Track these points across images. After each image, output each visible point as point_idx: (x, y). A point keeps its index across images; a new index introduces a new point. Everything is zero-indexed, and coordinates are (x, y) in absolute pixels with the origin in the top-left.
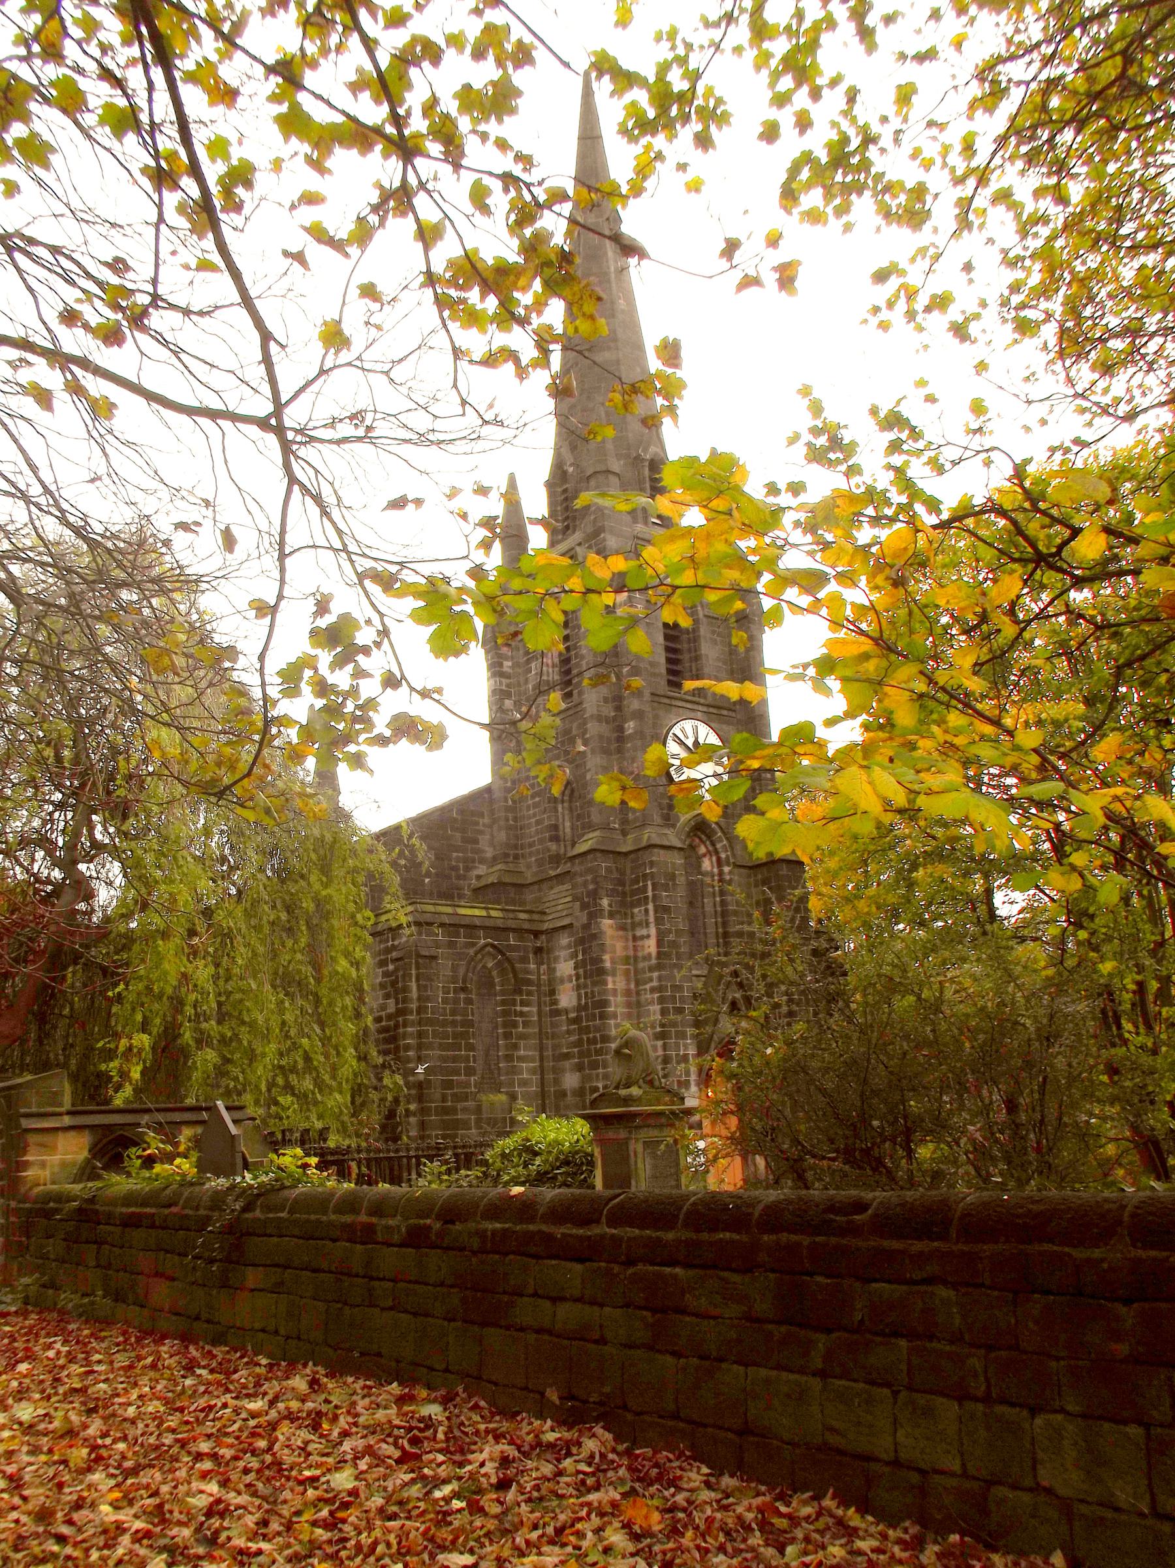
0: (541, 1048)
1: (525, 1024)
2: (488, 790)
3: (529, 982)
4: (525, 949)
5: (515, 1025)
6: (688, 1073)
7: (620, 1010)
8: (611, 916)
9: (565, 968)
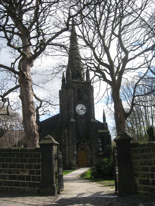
9: (63, 136)
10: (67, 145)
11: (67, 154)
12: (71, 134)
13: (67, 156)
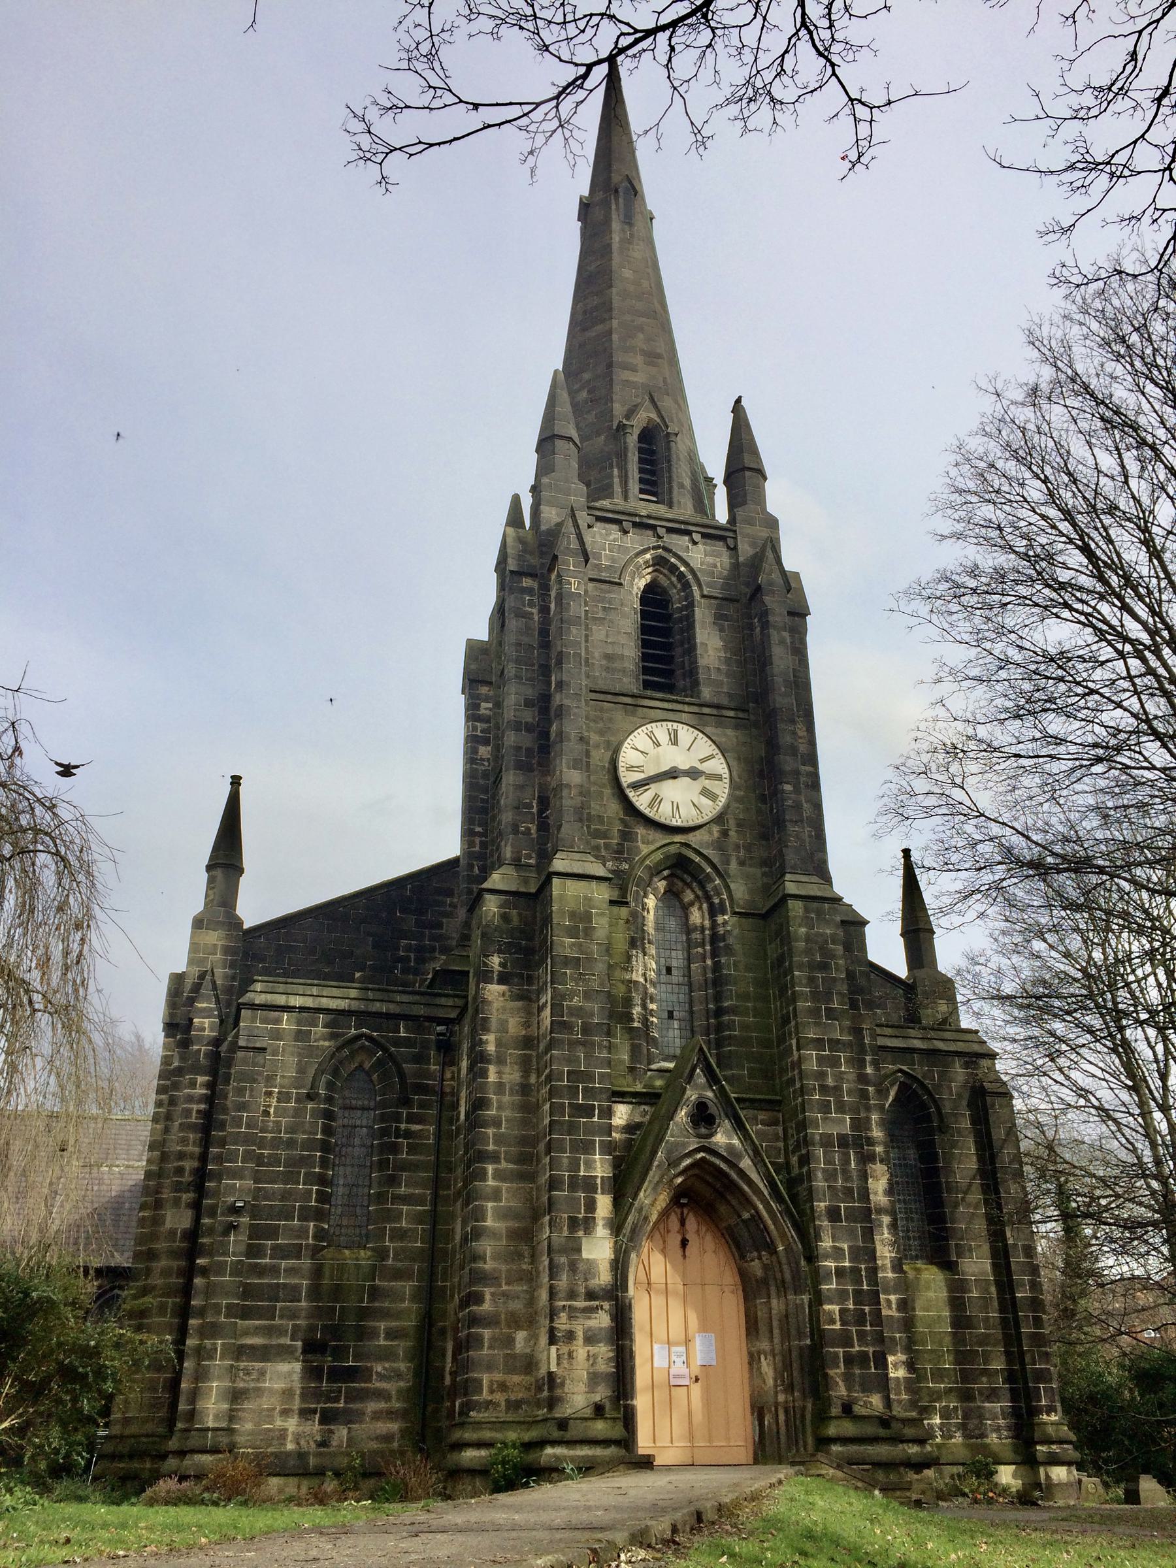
0: (437, 1184)
1: (412, 1149)
2: (454, 862)
3: (422, 1089)
4: (425, 1045)
5: (394, 1149)
6: (591, 1206)
7: (506, 1114)
8: (501, 981)
10: (495, 1158)
11: (489, 1265)
12: (548, 1022)
13: (488, 1292)
